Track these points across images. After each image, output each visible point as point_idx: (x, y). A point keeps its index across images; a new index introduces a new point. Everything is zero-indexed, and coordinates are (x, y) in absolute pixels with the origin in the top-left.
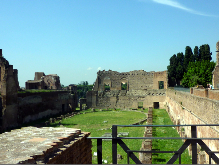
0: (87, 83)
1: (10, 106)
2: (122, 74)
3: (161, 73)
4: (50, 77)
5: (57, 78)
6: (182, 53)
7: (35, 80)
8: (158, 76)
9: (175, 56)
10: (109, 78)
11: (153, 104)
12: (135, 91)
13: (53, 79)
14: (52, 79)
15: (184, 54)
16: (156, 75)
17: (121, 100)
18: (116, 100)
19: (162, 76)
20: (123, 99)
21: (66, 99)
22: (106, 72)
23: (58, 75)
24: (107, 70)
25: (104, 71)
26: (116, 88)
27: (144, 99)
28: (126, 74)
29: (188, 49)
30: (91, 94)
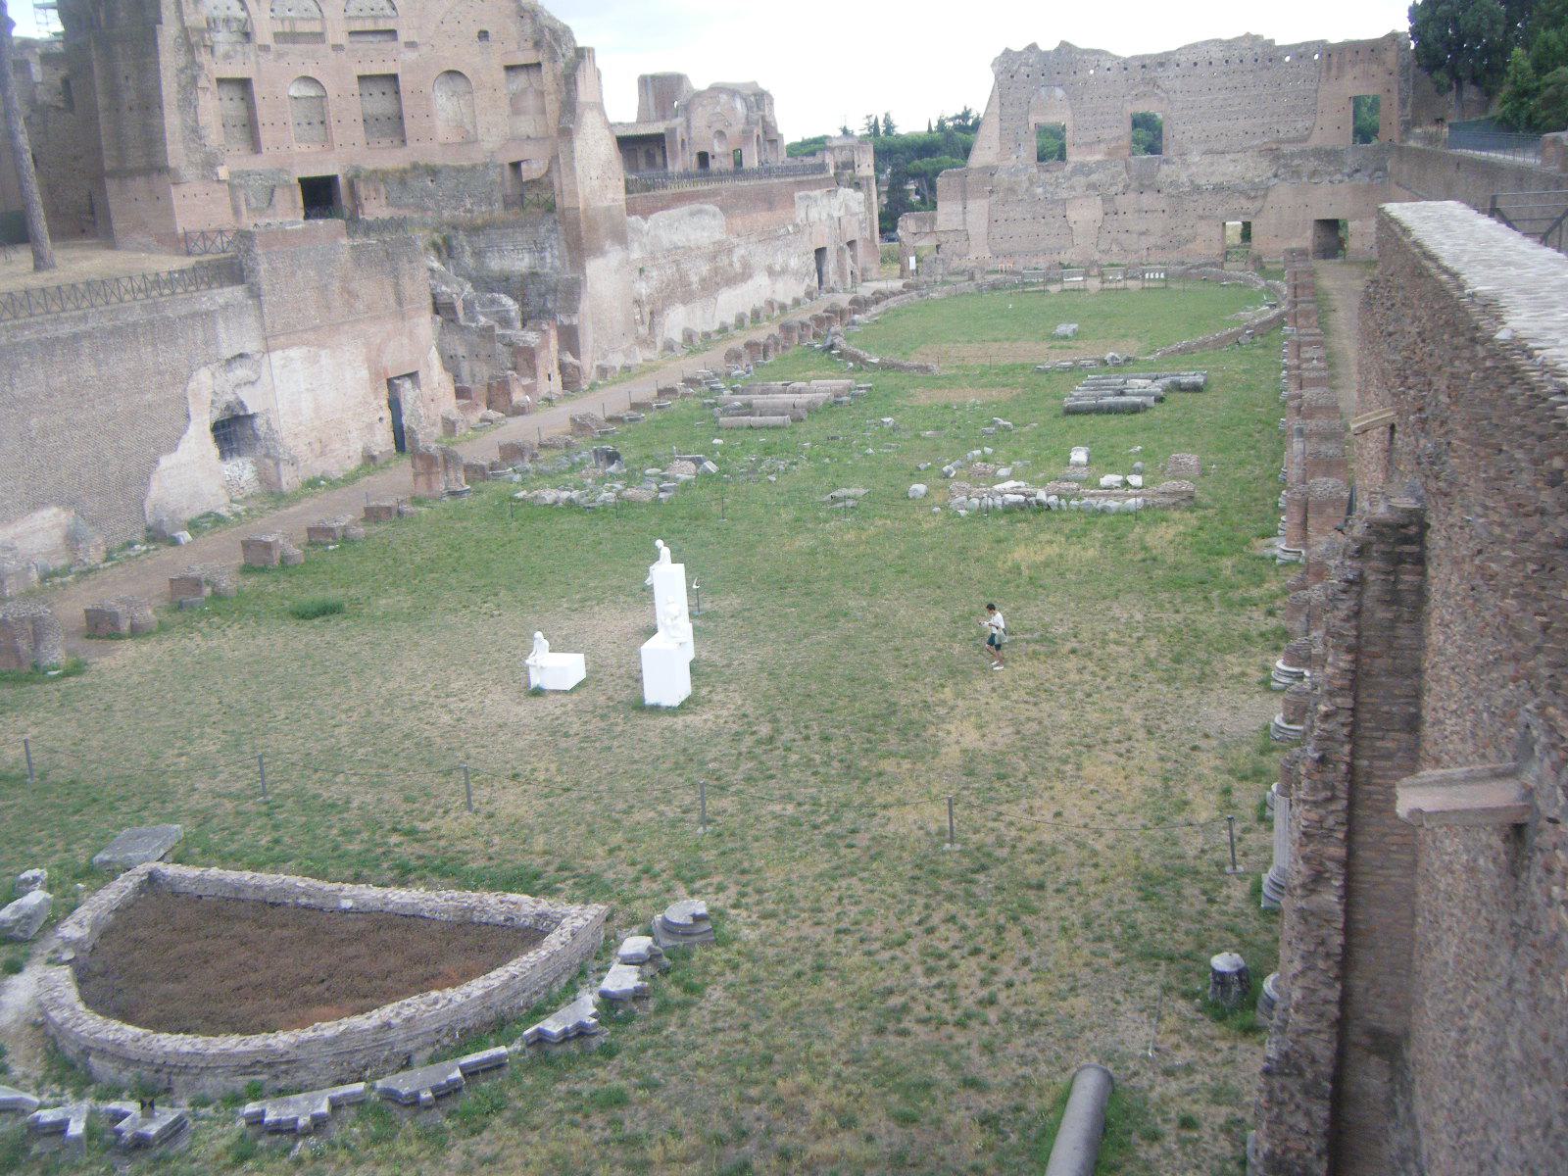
0: (889, 128)
4: (724, 98)
5: (759, 99)
7: (642, 119)
10: (1059, 93)
11: (1309, 233)
12: (1208, 159)
13: (739, 105)
14: (733, 109)
16: (1335, 59)
17: (1129, 216)
18: (1099, 214)
20: (1139, 211)
21: (830, 216)
22: (1047, 54)
23: (763, 86)
24: (1048, 45)
25: (1033, 47)
26: (1103, 146)
27: (1258, 204)
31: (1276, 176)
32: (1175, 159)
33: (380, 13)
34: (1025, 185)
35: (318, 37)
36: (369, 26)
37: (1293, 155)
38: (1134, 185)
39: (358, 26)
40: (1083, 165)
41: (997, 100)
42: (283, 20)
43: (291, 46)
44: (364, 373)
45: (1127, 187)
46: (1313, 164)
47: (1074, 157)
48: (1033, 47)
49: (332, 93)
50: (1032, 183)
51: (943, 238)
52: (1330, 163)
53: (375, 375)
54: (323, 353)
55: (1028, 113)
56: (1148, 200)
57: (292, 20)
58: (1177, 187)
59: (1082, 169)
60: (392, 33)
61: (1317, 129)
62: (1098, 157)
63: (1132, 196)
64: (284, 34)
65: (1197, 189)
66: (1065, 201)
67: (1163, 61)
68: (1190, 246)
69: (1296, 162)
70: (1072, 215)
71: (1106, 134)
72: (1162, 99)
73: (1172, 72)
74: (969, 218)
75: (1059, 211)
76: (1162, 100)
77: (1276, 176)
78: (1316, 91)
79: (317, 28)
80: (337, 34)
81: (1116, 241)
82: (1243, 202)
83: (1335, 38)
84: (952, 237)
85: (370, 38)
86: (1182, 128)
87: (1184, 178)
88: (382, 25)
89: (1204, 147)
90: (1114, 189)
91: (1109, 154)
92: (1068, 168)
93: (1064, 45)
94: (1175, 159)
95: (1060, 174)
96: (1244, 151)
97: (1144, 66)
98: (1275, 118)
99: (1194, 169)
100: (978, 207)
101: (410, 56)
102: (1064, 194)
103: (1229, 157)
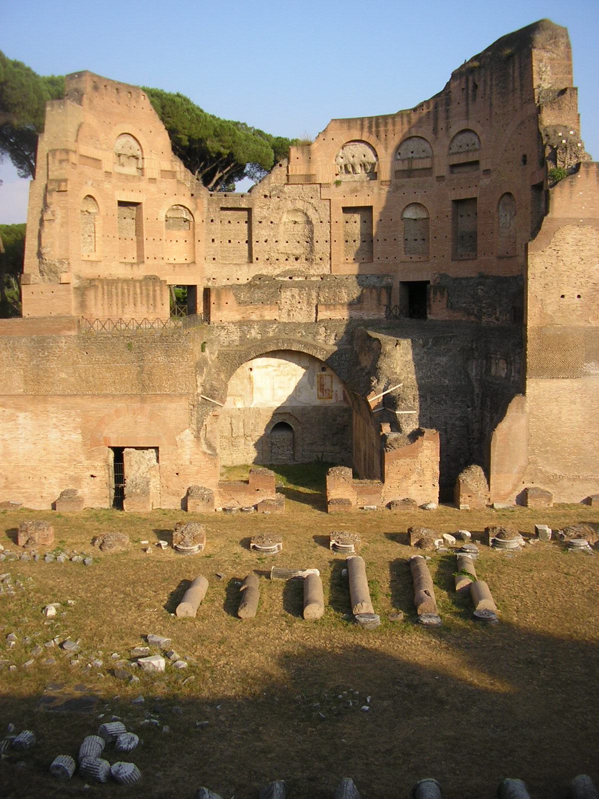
1: (566, 383)
33: (471, 148)
35: (428, 171)
36: (462, 159)
39: (456, 160)
42: (403, 160)
43: (407, 179)
44: (77, 437)
49: (432, 217)
53: (91, 441)
54: (22, 415)
57: (410, 160)
60: (476, 163)
64: (404, 171)
79: (426, 164)
80: (441, 169)
85: (468, 169)
88: (471, 158)
101: (485, 181)
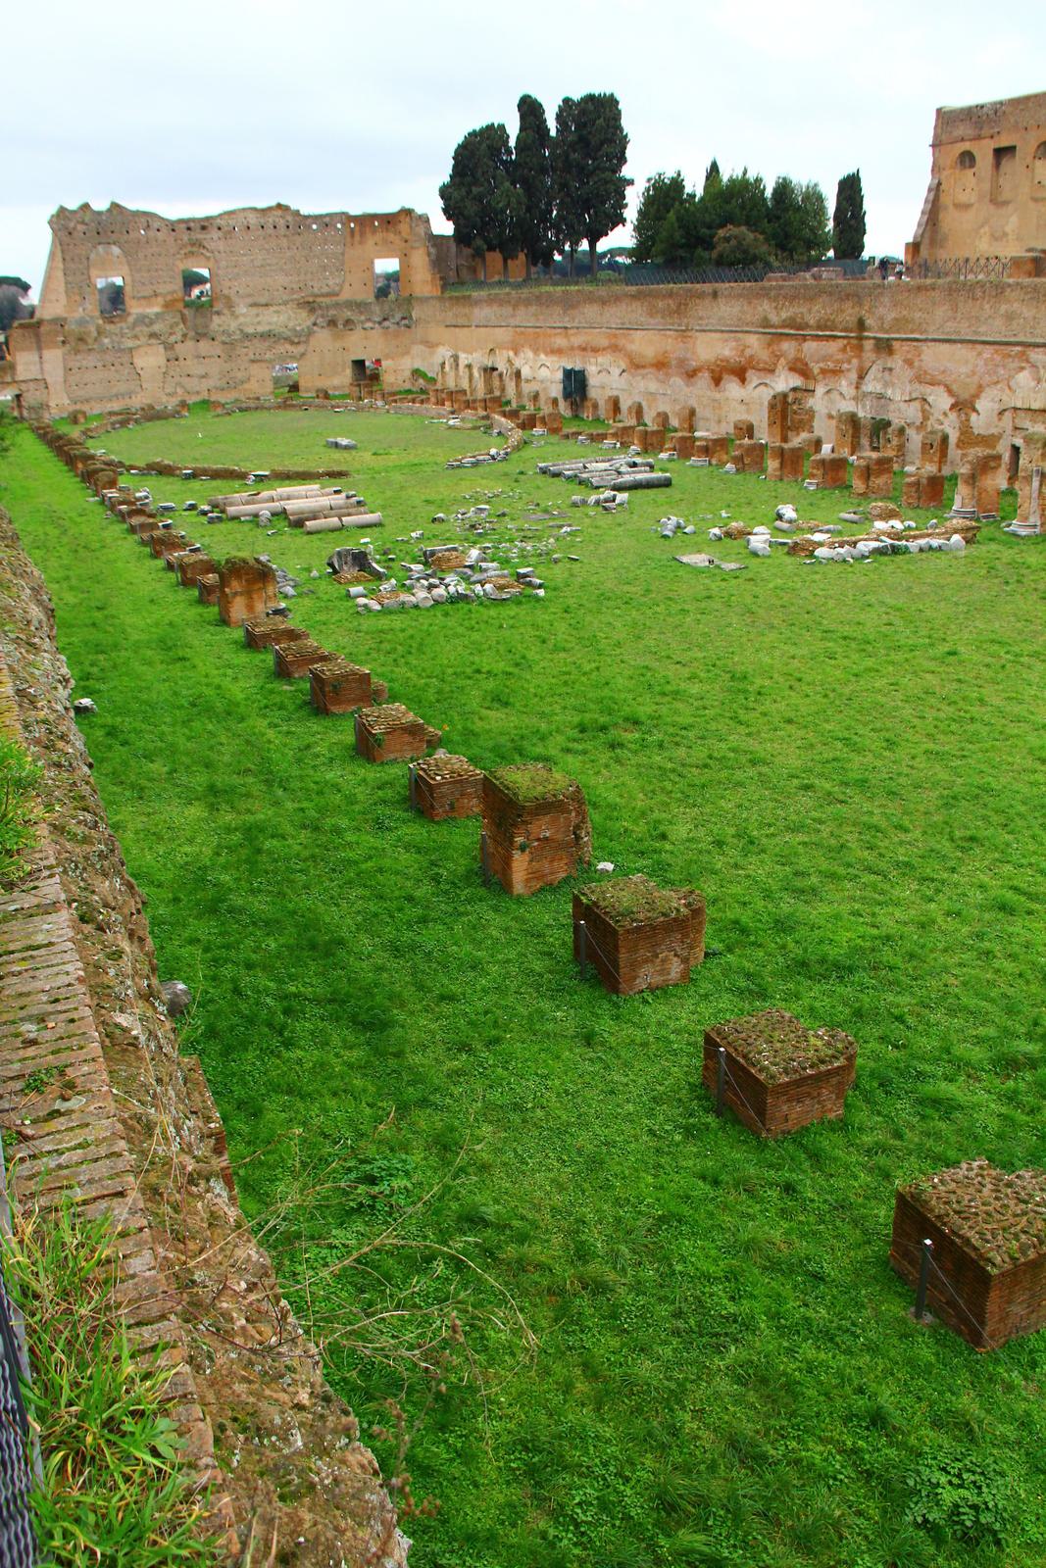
2: (184, 226)
3: (389, 221)
6: (502, 127)
8: (369, 235)
9: (473, 134)
10: (116, 250)
11: (349, 372)
12: (254, 310)
15: (513, 130)
17: (188, 362)
18: (162, 361)
19: (391, 236)
20: (198, 357)
22: (99, 213)
24: (100, 205)
25: (86, 207)
26: (160, 300)
27: (301, 349)
28: (204, 228)
29: (529, 109)
30: (38, 336)
31: (315, 324)
32: (226, 311)
34: (95, 334)
37: (328, 308)
38: (192, 334)
40: (145, 316)
41: (59, 254)
45: (185, 336)
46: (348, 314)
47: (135, 309)
48: (86, 207)
50: (99, 333)
51: (24, 387)
52: (361, 313)
55: (88, 268)
56: (204, 346)
58: (229, 335)
59: (143, 320)
61: (347, 285)
62: (157, 309)
63: (190, 344)
65: (247, 336)
66: (131, 349)
67: (205, 224)
68: (246, 386)
69: (332, 312)
70: (139, 362)
71: (163, 289)
72: (208, 258)
73: (215, 234)
74: (47, 367)
75: (125, 359)
76: (208, 258)
77: (315, 324)
78: (343, 254)
81: (179, 384)
82: (288, 347)
83: (354, 212)
84: (32, 385)
86: (228, 284)
87: (233, 325)
89: (250, 300)
90: (173, 339)
91: (167, 305)
92: (131, 319)
93: (115, 206)
94: (226, 311)
95: (123, 325)
96: (285, 303)
97: (189, 229)
98: (309, 276)
99: (242, 319)
100: (54, 357)
102: (130, 344)
103: (275, 308)
